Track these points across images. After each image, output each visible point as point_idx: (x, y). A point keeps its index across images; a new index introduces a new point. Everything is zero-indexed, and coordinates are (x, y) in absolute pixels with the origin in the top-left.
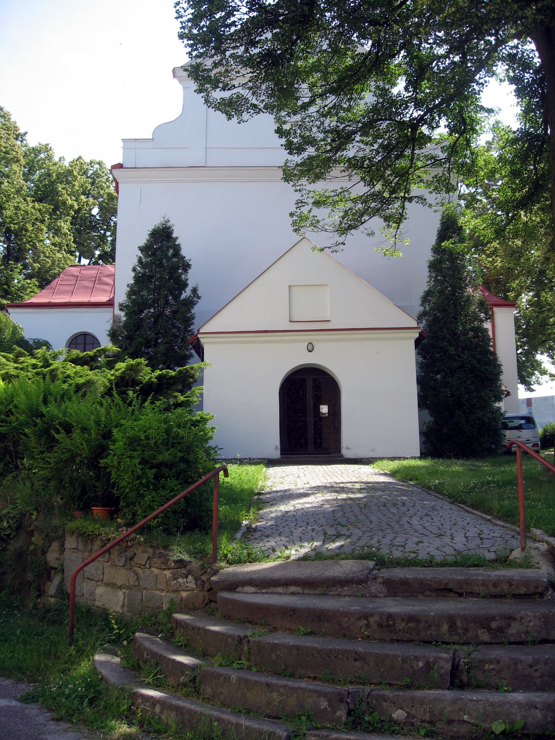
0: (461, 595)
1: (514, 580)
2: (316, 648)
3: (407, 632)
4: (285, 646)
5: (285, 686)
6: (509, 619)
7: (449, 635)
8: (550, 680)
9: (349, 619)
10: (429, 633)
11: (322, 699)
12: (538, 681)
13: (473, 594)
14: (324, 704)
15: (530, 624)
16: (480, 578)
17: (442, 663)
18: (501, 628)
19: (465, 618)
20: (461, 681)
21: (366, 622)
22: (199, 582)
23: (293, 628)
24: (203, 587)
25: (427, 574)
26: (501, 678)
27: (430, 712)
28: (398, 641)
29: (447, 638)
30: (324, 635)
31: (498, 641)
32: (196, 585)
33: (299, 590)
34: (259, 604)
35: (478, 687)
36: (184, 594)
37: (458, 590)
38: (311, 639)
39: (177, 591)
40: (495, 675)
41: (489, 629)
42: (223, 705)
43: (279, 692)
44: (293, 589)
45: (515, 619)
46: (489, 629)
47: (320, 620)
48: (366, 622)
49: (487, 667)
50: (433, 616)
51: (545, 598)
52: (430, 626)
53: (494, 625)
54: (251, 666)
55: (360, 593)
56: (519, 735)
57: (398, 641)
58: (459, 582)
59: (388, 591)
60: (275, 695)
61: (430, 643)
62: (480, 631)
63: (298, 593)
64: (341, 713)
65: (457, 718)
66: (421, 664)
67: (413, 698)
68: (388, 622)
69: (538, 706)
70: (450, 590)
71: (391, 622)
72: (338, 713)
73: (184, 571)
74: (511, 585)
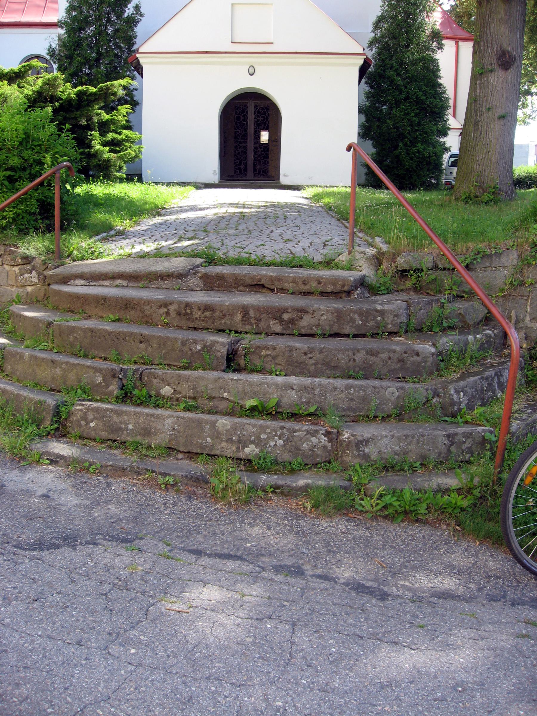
0: (272, 290)
1: (322, 278)
2: (106, 331)
3: (203, 321)
4: (81, 329)
5: (67, 363)
6: (300, 312)
7: (243, 324)
8: (324, 368)
9: (151, 307)
10: (223, 321)
11: (97, 374)
12: (312, 368)
13: (283, 291)
14: (99, 379)
15: (323, 318)
16: (291, 275)
17: (218, 347)
18: (293, 319)
19: (258, 309)
20: (239, 365)
21: (166, 310)
22: (41, 277)
23: (104, 316)
24: (44, 282)
25: (243, 270)
26: (276, 364)
27: (193, 389)
28: (195, 328)
29: (240, 328)
30: (131, 321)
31: (289, 333)
32: (39, 280)
33: (124, 283)
34: (77, 294)
35: (252, 371)
36: (29, 289)
37: (269, 286)
38: (117, 324)
39: (23, 286)
40: (271, 361)
41: (281, 321)
42: (19, 380)
43: (61, 367)
44: (119, 282)
45: (307, 312)
46: (281, 321)
47: (127, 308)
48: (166, 310)
49: (263, 353)
50: (227, 306)
51: (352, 297)
52: (225, 315)
53: (286, 317)
54: (53, 348)
55: (178, 286)
56: (274, 413)
57: (195, 328)
58: (271, 279)
59: (205, 285)
60: (58, 371)
61: (224, 331)
62: (272, 322)
63: (123, 286)
64: (114, 388)
65: (217, 395)
66: (199, 347)
67: (179, 376)
68: (186, 310)
69: (294, 387)
70: (263, 286)
71: (188, 311)
72: (111, 388)
73: (29, 267)
74: (319, 283)
